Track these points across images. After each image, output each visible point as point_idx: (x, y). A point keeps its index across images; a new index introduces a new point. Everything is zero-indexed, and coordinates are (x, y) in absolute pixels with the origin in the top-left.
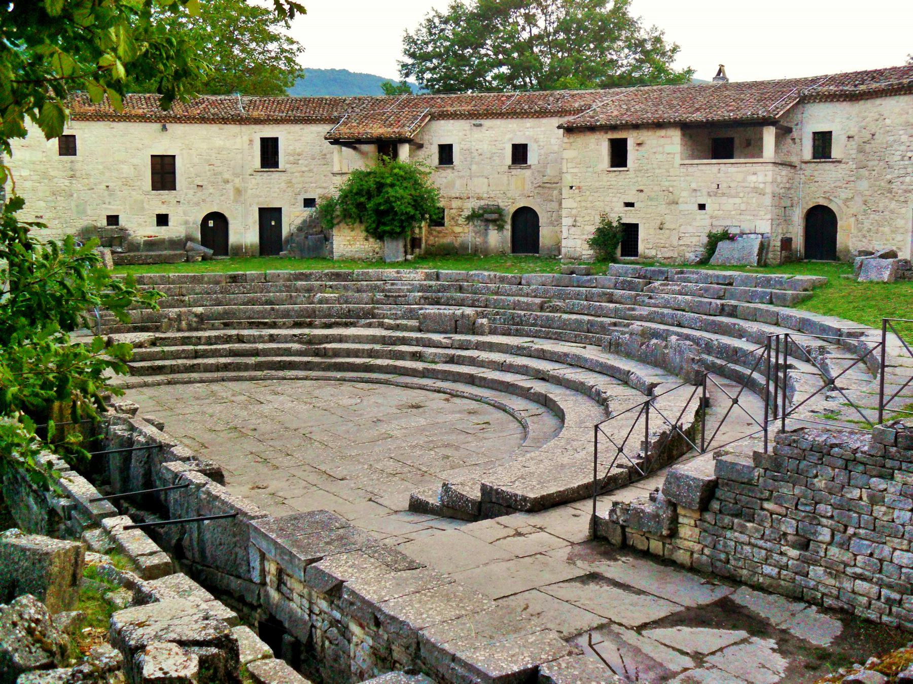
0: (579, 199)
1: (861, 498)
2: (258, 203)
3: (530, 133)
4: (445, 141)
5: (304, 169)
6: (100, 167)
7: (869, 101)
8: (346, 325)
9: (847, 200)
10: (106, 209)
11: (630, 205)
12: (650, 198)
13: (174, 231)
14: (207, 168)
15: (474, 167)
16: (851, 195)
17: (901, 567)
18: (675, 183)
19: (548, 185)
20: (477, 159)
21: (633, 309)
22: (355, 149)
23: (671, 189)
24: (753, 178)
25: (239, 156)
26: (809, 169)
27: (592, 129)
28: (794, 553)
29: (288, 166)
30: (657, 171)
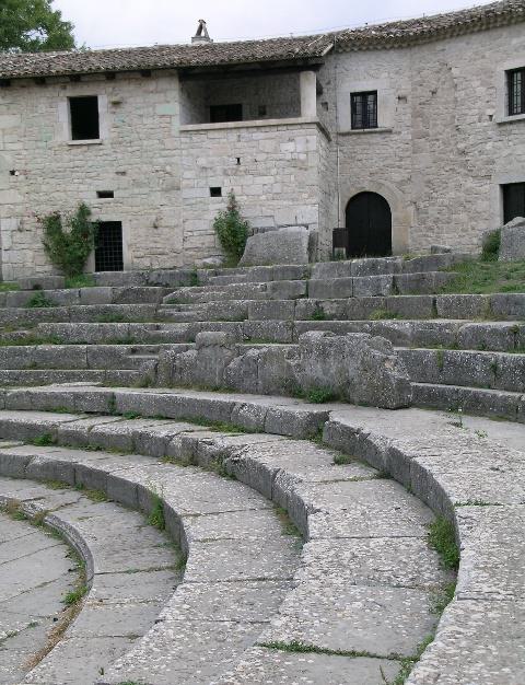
0: (26, 189)
7: (424, 48)
9: (401, 183)
11: (107, 194)
12: (137, 184)
16: (407, 176)
18: (173, 160)
23: (168, 168)
24: (290, 146)
26: (349, 144)
27: (41, 80)
30: (145, 143)
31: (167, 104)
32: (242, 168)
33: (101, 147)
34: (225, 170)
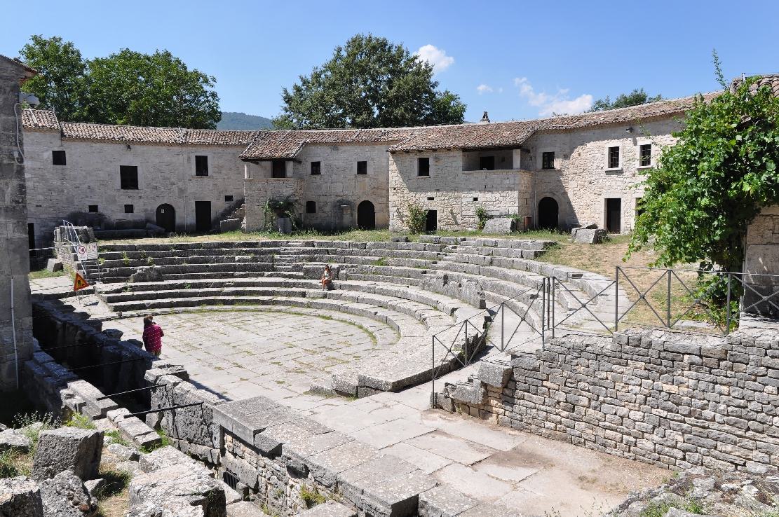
1: (607, 379)
3: (368, 154)
4: (316, 160)
6: (84, 173)
8: (257, 276)
10: (89, 201)
13: (138, 214)
17: (635, 421)
20: (335, 171)
21: (436, 263)
22: (257, 164)
24: (507, 181)
25: (181, 168)
28: (565, 414)
29: (214, 175)
31: (458, 160)
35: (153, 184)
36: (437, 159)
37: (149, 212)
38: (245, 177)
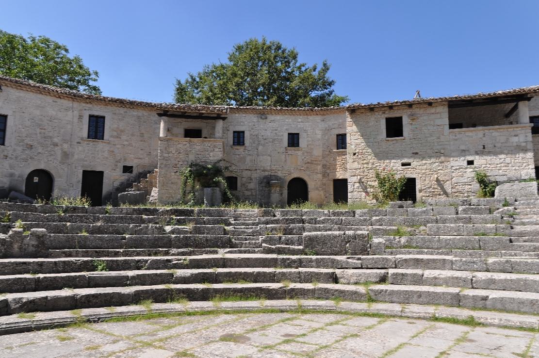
2: (82, 166)
3: (301, 125)
4: (239, 128)
5: (126, 143)
14: (38, 131)
15: (260, 148)
19: (314, 162)
20: (262, 142)
23: (442, 151)
24: (515, 139)
25: (69, 127)
30: (429, 139)
31: (443, 117)
32: (486, 150)
33: (404, 141)
34: (476, 151)
35: (28, 141)
36: (413, 117)
37: (16, 178)
38: (161, 135)
